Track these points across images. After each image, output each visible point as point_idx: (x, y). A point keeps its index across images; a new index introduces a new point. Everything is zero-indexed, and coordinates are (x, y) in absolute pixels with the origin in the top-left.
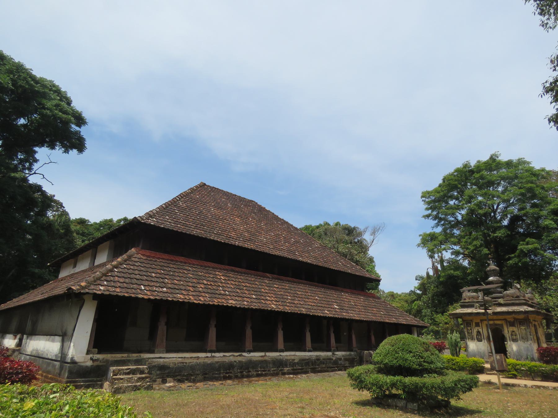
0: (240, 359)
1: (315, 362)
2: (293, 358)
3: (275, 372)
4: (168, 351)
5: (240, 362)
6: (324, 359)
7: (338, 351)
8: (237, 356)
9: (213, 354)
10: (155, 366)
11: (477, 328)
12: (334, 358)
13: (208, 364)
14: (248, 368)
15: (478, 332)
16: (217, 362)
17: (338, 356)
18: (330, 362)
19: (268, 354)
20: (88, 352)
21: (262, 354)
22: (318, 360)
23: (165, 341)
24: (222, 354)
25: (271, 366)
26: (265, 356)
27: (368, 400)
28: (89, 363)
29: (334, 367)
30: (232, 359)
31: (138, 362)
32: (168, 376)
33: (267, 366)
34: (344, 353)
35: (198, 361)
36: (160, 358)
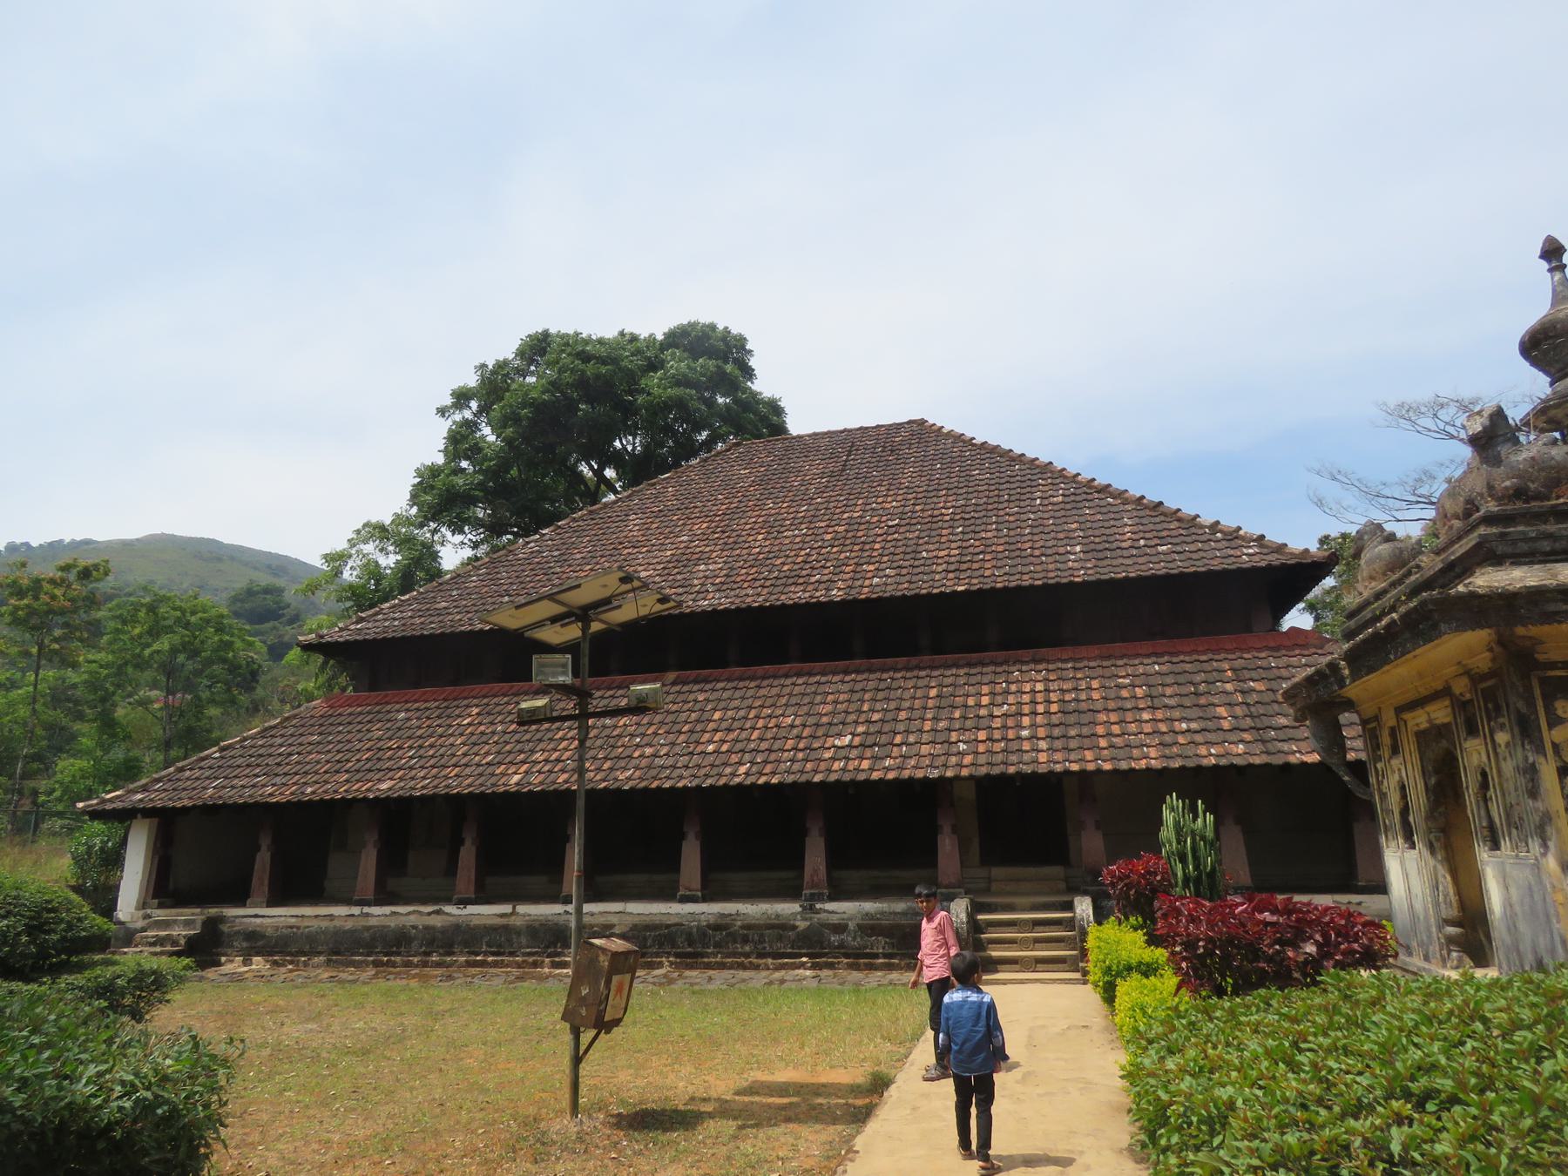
0: (437, 921)
1: (705, 935)
2: (614, 920)
3: (531, 959)
4: (270, 904)
5: (426, 928)
6: (748, 927)
7: (832, 899)
8: (429, 914)
9: (366, 909)
10: (238, 932)
11: (1396, 762)
12: (802, 925)
13: (345, 932)
14: (451, 946)
15: (1403, 788)
16: (368, 928)
17: (834, 919)
18: (780, 938)
19: (521, 909)
20: (143, 905)
21: (506, 908)
22: (717, 927)
23: (266, 882)
24: (387, 910)
25: (524, 941)
26: (513, 913)
27: (859, 1086)
28: (140, 924)
29: (802, 956)
30: (413, 919)
31: (188, 924)
32: (258, 954)
33: (509, 941)
34: (869, 906)
35: (324, 924)
36: (256, 916)
